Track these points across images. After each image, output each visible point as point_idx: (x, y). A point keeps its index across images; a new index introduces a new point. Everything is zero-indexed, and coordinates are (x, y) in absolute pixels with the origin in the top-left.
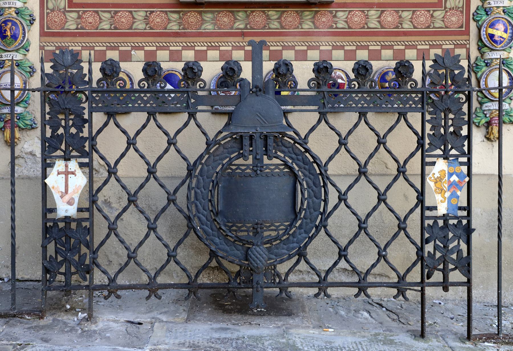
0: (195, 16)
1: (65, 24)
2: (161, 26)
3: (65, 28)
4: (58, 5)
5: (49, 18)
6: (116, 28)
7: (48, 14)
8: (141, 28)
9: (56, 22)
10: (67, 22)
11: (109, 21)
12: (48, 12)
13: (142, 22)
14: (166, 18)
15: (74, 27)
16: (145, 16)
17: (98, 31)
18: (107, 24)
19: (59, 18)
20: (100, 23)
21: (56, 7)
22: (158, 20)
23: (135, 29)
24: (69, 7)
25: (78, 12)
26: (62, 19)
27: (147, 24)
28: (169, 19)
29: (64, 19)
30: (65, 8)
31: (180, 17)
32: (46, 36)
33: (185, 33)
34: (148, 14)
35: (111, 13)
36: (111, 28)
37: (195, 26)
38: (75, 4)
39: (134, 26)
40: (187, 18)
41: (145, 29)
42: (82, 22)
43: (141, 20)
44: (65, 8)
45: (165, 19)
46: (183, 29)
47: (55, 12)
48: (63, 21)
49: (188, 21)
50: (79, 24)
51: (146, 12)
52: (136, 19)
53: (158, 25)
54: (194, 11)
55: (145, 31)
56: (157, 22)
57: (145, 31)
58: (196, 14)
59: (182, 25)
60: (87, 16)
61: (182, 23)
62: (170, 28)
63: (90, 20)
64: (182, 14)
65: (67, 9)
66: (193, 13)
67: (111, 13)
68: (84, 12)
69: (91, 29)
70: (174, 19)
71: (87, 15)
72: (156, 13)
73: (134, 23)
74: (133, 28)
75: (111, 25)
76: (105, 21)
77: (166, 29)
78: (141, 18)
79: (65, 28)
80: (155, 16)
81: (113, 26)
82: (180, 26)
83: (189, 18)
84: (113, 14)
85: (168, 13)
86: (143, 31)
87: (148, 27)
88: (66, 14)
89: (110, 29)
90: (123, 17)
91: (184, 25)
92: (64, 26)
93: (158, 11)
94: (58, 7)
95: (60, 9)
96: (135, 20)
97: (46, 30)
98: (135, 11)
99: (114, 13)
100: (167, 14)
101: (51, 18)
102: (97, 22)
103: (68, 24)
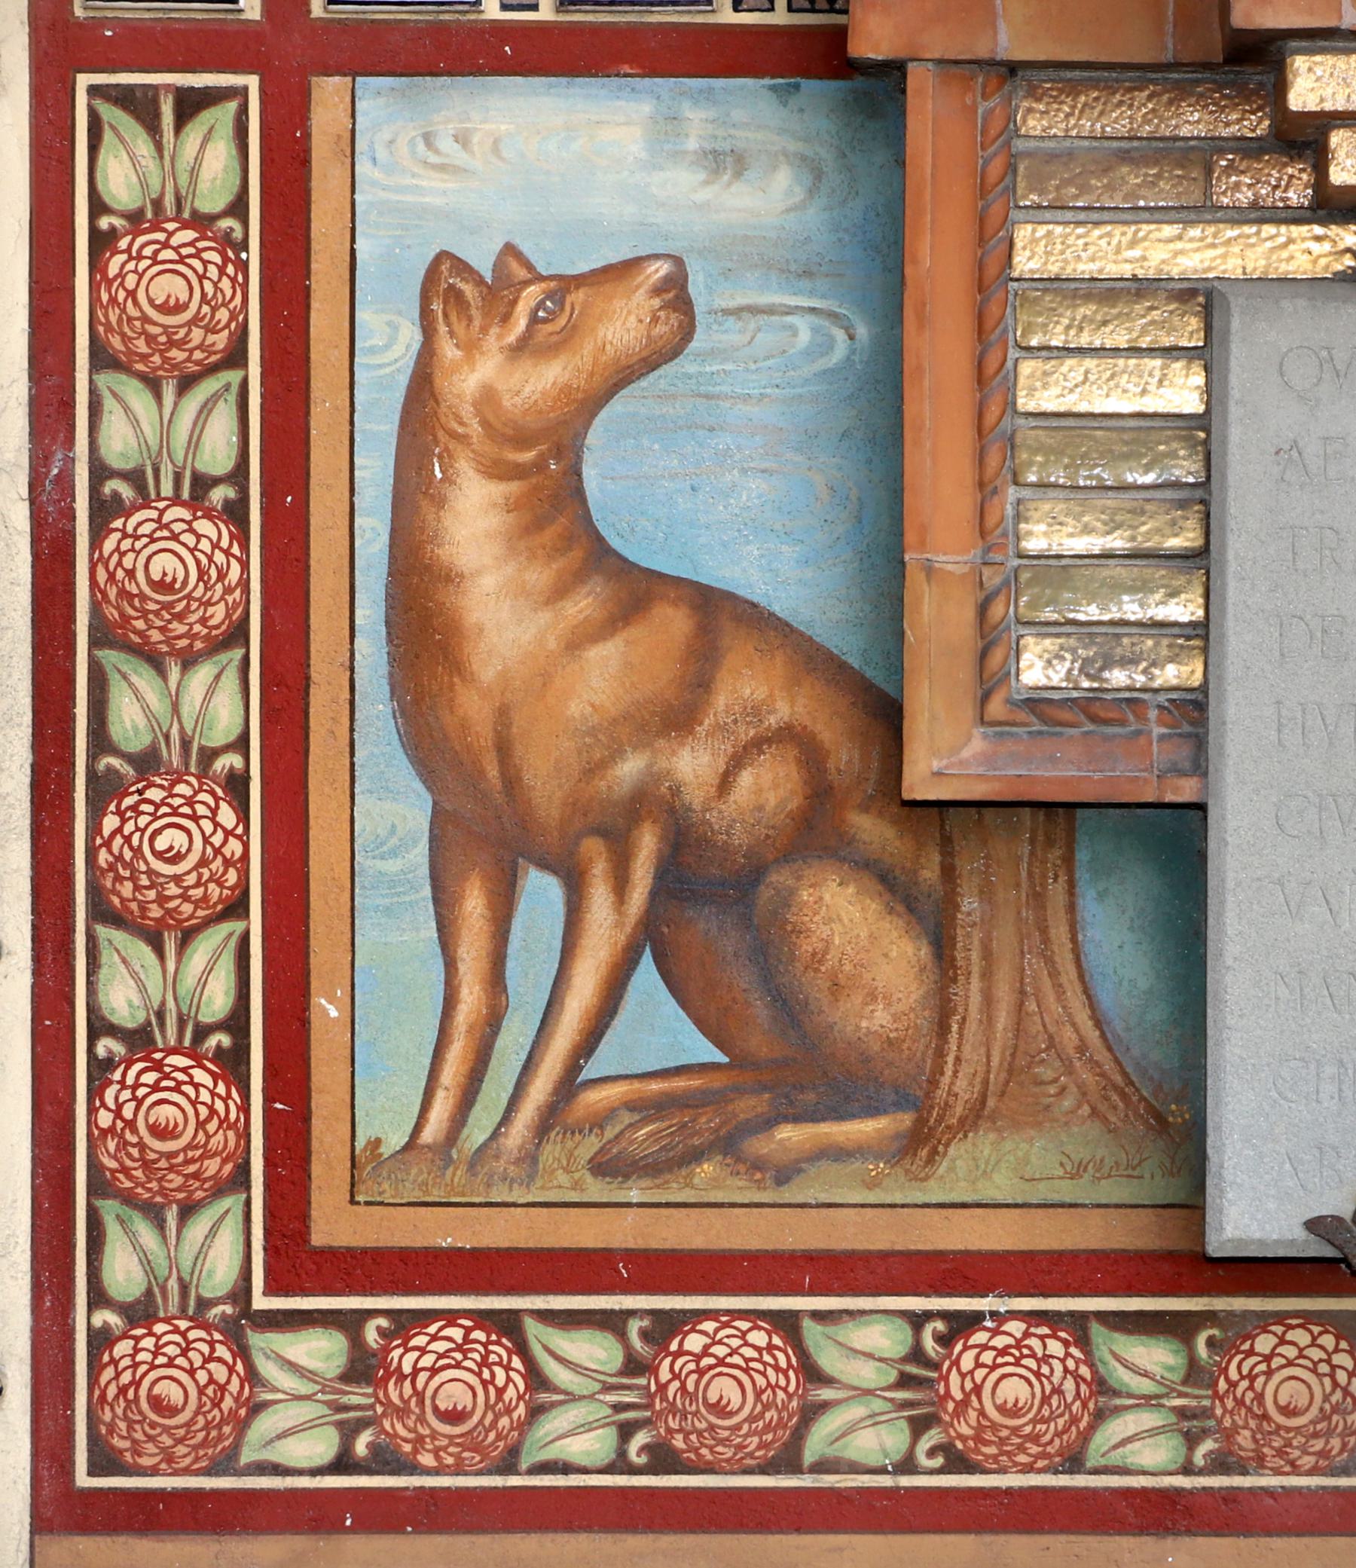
0: (1316, 1354)
1: (242, 1426)
2: (1035, 1438)
3: (246, 1457)
4: (186, 1264)
5: (108, 1373)
6: (662, 1459)
7: (101, 1340)
8: (874, 1460)
9: (173, 1411)
10: (257, 1408)
11: (612, 1398)
12: (106, 1328)
13: (878, 1405)
14: (1078, 1378)
15: (321, 1446)
16: (905, 1360)
17: (514, 1481)
18: (588, 1427)
19: (191, 1372)
20: (536, 1412)
21: (173, 1285)
22: (1014, 1390)
23: (819, 1467)
24: (273, 1288)
25: (350, 1323)
26: (223, 1388)
27: (919, 1426)
28: (1101, 1386)
29: (234, 1386)
30: (241, 1293)
31: (1193, 1362)
32: (84, 1527)
33: (1231, 1496)
34: (929, 1344)
35: (622, 1336)
36: (622, 1453)
37: (1318, 1445)
38: (331, 1254)
39: (815, 1446)
40: (1252, 1378)
41: (907, 1465)
42: (388, 1404)
43: (869, 1392)
44: (241, 1293)
45: (1069, 1385)
46: (1220, 1464)
47: (160, 1328)
48: (228, 1403)
49: (1260, 1397)
50: (361, 1425)
51: (917, 1321)
52: (827, 1381)
53: (1015, 1431)
54: (1308, 1318)
55: (905, 1481)
56: (1001, 1409)
57: (905, 1481)
58: (1328, 1341)
59: (1205, 1433)
60: (427, 1361)
61: (1206, 1413)
62: (1115, 1458)
63: (454, 1391)
64: (1211, 1343)
65: (260, 1302)
66: (1301, 1337)
67: (622, 1336)
68: (405, 1324)
69: (458, 1470)
70: (1146, 1386)
71: (423, 1351)
72: (996, 1332)
73: (812, 1412)
74: (809, 1457)
75: (626, 1431)
76: (572, 1398)
77: (1074, 1462)
78: (868, 1374)
79: (246, 1457)
80: (987, 1357)
81: (641, 1439)
82: (1191, 1440)
83: (1269, 1373)
84: (637, 1343)
85: (1096, 1330)
86: (885, 1481)
87: (931, 1453)
88: (257, 1340)
89: (619, 1464)
90: (721, 1362)
91: (1229, 1435)
92: (237, 1446)
93: (1013, 1315)
94: (184, 1288)
95: (204, 1304)
96: (826, 1394)
97: (83, 1479)
98: (818, 1316)
99: (644, 1335)
100: (1083, 1341)
101: (126, 1378)
102: (509, 1411)
103: (264, 1425)
